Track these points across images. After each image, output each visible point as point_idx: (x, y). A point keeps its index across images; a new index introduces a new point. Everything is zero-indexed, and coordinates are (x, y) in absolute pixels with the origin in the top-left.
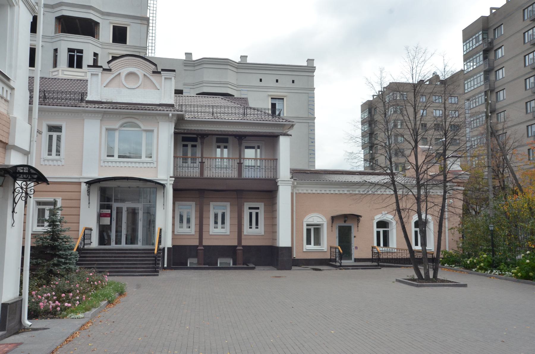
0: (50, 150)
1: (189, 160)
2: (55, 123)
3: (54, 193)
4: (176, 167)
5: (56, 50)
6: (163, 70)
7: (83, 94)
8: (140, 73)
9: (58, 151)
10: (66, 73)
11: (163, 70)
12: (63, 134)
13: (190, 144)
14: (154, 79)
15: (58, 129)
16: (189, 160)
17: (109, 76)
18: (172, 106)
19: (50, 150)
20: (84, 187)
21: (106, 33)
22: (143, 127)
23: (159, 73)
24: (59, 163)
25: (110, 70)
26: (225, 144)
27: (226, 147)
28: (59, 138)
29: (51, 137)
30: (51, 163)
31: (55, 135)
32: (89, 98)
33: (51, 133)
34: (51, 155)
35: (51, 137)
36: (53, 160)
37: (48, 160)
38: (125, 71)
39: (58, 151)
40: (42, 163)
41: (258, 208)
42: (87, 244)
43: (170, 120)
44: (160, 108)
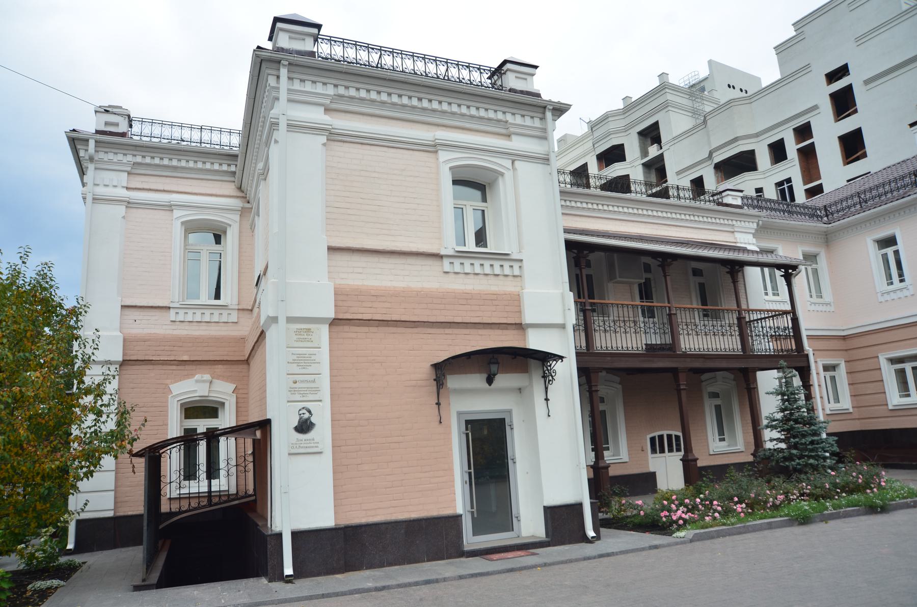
0: (889, 277)
3: (908, 342)
9: (901, 275)
12: (900, 246)
15: (890, 241)
19: (889, 277)
24: (906, 293)
28: (897, 253)
30: (893, 296)
31: (890, 251)
33: (884, 251)
34: (892, 283)
36: (895, 291)
37: (888, 293)
39: (901, 275)
40: (881, 299)
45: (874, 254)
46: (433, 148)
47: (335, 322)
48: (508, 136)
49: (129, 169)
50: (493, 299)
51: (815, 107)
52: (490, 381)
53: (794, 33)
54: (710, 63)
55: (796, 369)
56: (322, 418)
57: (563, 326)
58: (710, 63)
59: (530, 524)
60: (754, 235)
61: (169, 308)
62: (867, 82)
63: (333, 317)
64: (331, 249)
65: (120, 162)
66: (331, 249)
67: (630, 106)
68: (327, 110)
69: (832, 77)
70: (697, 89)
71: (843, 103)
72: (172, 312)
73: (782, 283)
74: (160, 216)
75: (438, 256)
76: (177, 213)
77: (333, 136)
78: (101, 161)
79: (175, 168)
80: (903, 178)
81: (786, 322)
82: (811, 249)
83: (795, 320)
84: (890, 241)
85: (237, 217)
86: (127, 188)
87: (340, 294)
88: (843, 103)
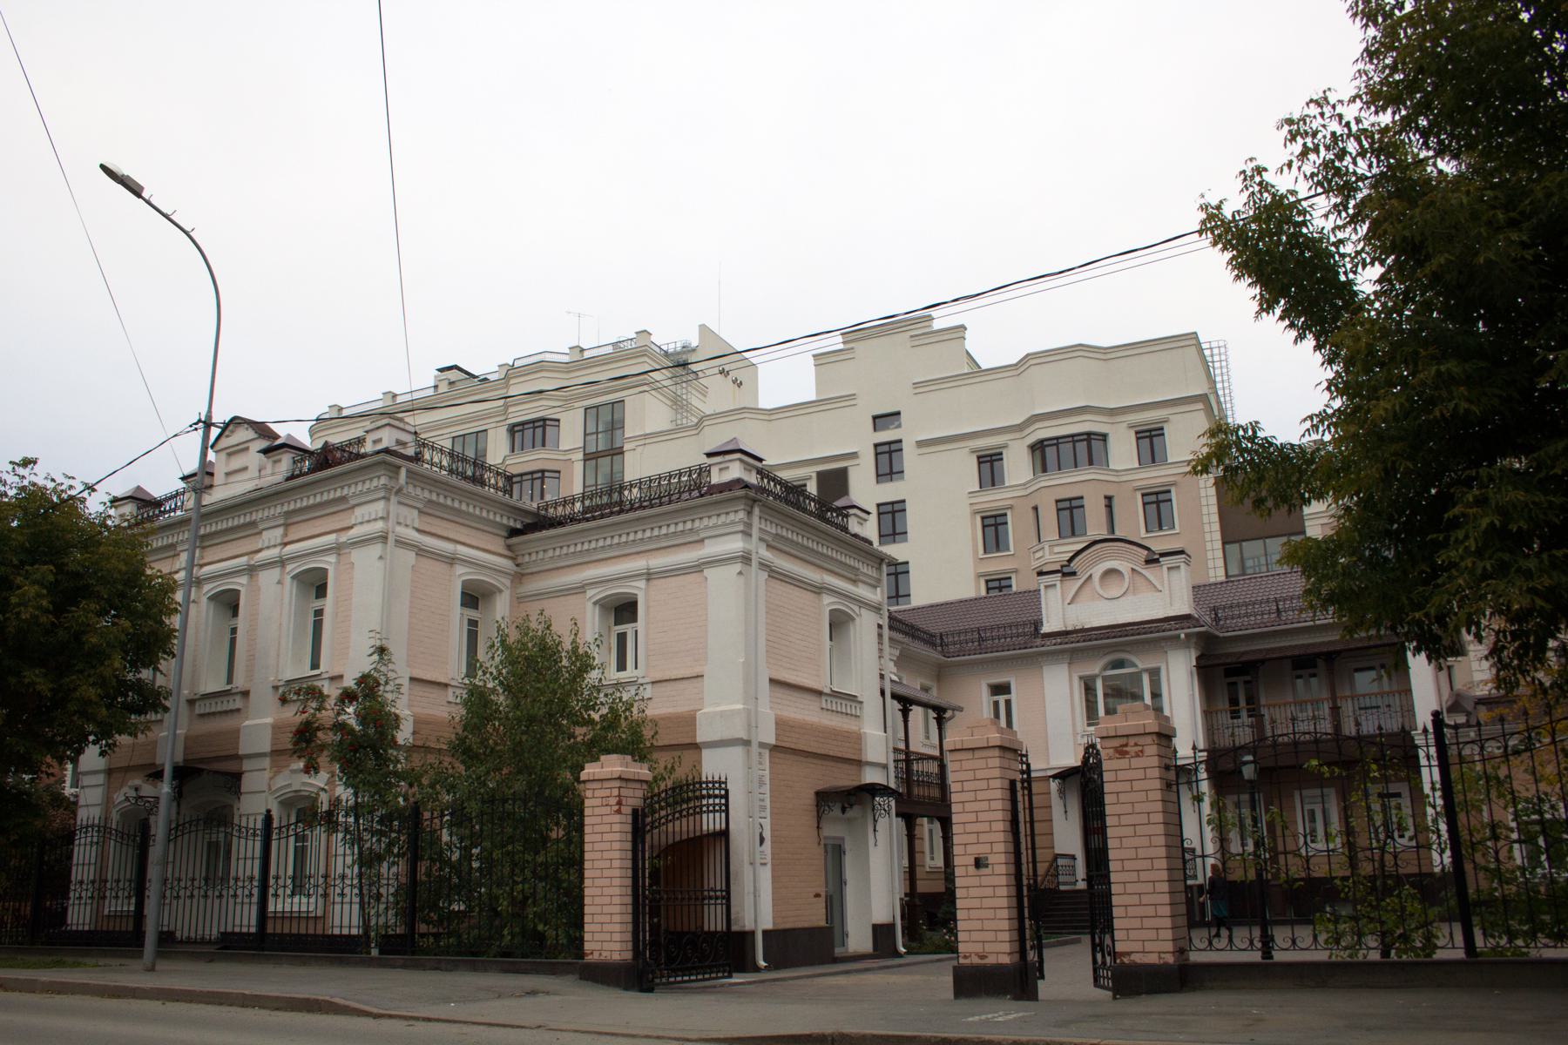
1: (1244, 714)
2: (998, 679)
4: (1210, 730)
5: (1036, 509)
6: (1162, 555)
7: (1037, 624)
8: (1123, 566)
10: (1057, 549)
11: (1162, 555)
12: (1013, 696)
13: (1240, 680)
14: (1149, 573)
16: (1244, 714)
17: (1073, 585)
18: (1187, 617)
20: (1054, 785)
21: (1123, 451)
22: (1141, 666)
23: (1157, 561)
25: (1074, 574)
26: (1311, 671)
27: (1314, 675)
28: (1008, 703)
29: (996, 704)
31: (1002, 699)
32: (1046, 629)
35: (996, 704)
38: (1098, 571)
41: (1398, 795)
42: (1065, 884)
43: (1185, 644)
44: (1166, 625)
45: (985, 699)
46: (819, 590)
47: (775, 749)
48: (854, 582)
49: (420, 506)
50: (835, 734)
51: (854, 455)
52: (844, 810)
53: (841, 346)
54: (703, 328)
55: (939, 819)
56: (767, 834)
57: (885, 767)
58: (703, 328)
59: (858, 939)
60: (896, 664)
61: (446, 685)
62: (921, 444)
63: (773, 741)
64: (772, 681)
65: (416, 498)
66: (772, 681)
67: (580, 360)
68: (769, 546)
69: (880, 421)
70: (680, 363)
71: (888, 460)
72: (450, 690)
73: (933, 725)
74: (440, 568)
75: (819, 693)
76: (460, 570)
77: (775, 574)
78: (408, 495)
79: (458, 512)
80: (1025, 624)
81: (933, 768)
82: (928, 683)
83: (942, 767)
84: (1001, 689)
85: (507, 582)
86: (418, 531)
87: (781, 725)
88: (888, 460)
